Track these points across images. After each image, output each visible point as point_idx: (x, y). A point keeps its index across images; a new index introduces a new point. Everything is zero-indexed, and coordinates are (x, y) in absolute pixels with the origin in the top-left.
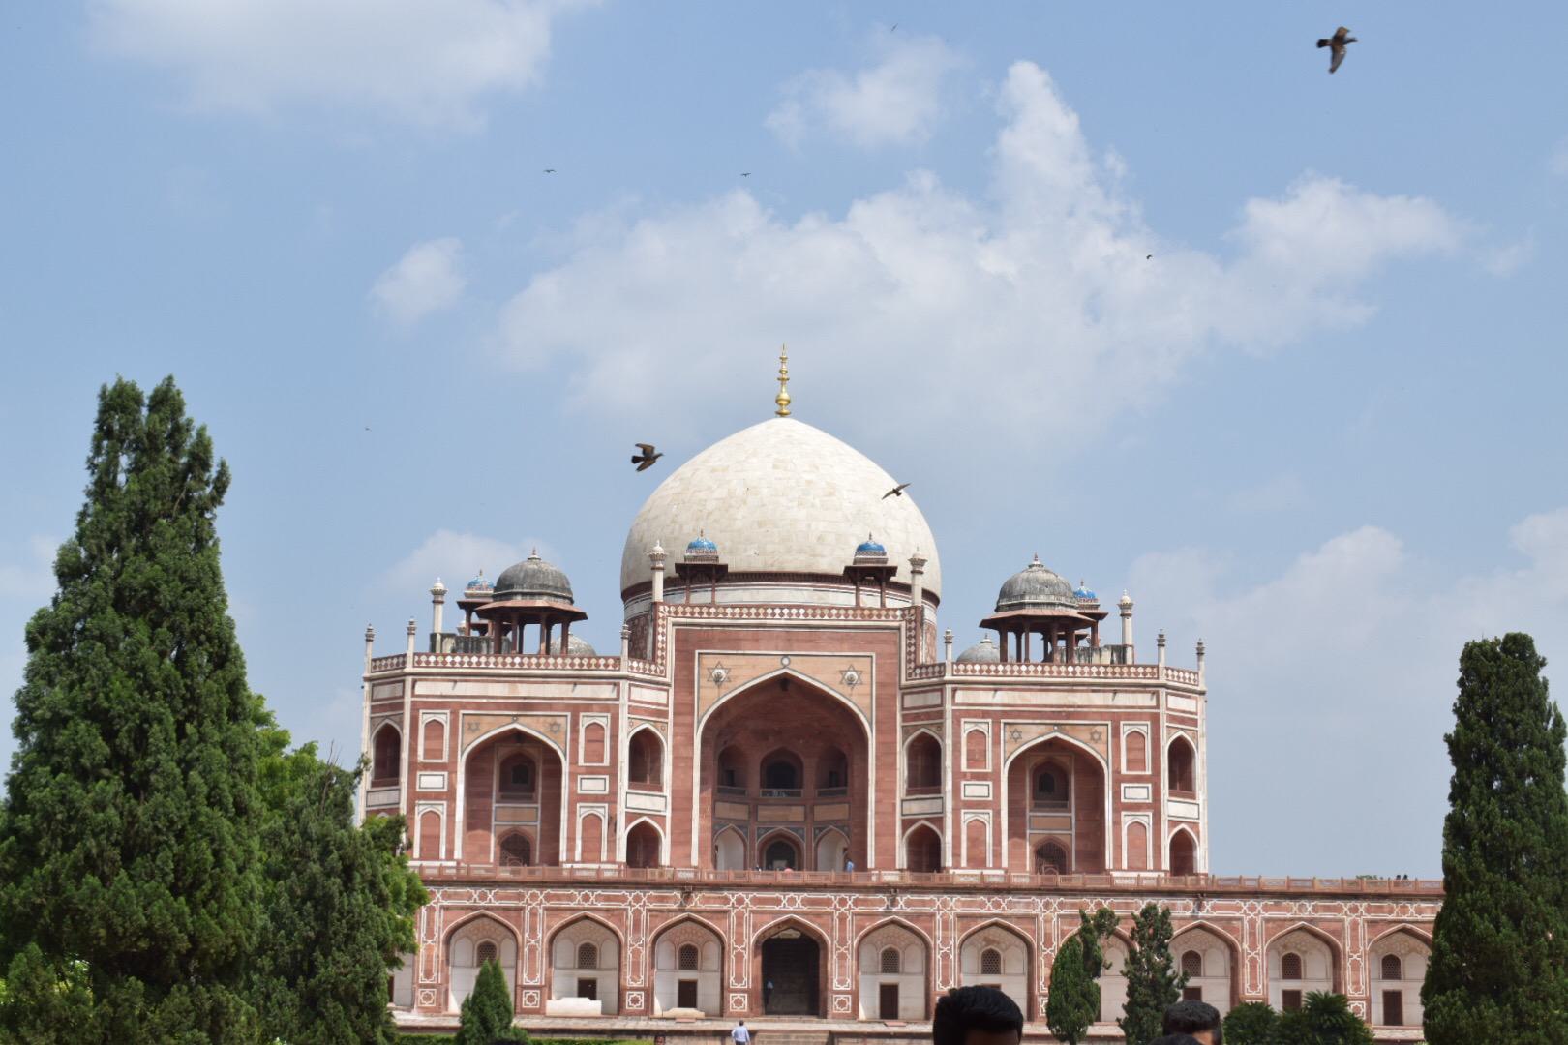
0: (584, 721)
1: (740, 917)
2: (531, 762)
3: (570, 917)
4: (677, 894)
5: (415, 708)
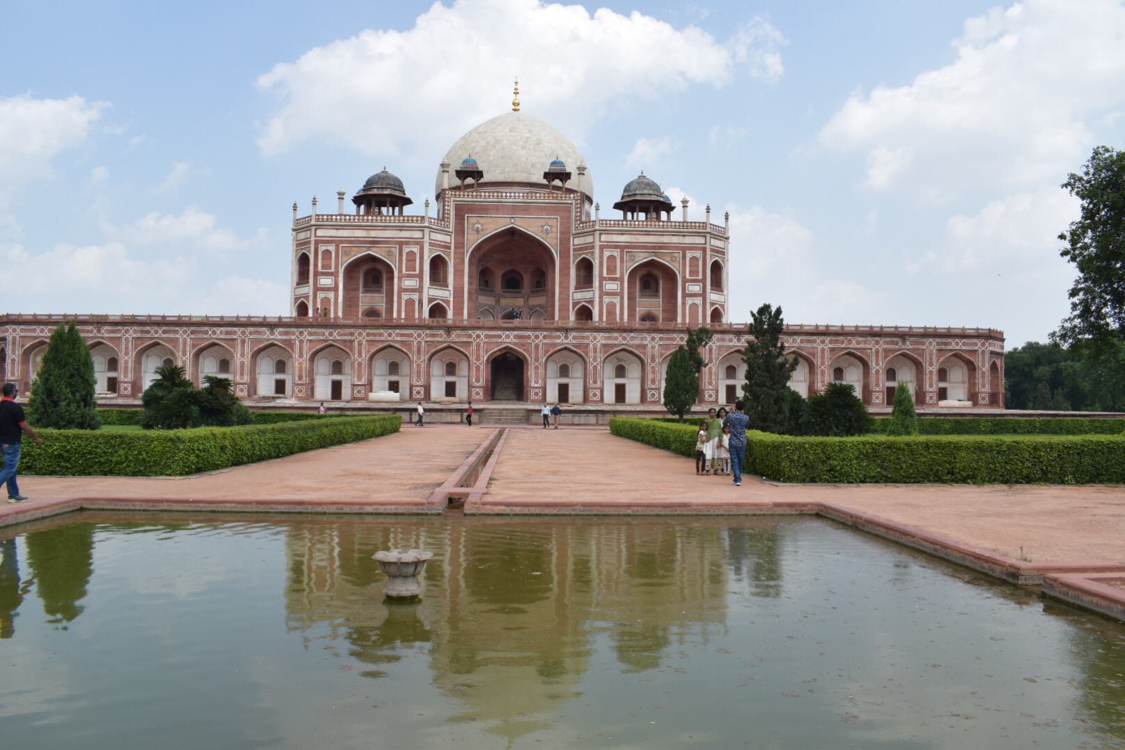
0: (406, 250)
1: (478, 345)
2: (380, 273)
3: (381, 346)
4: (441, 332)
5: (317, 243)
